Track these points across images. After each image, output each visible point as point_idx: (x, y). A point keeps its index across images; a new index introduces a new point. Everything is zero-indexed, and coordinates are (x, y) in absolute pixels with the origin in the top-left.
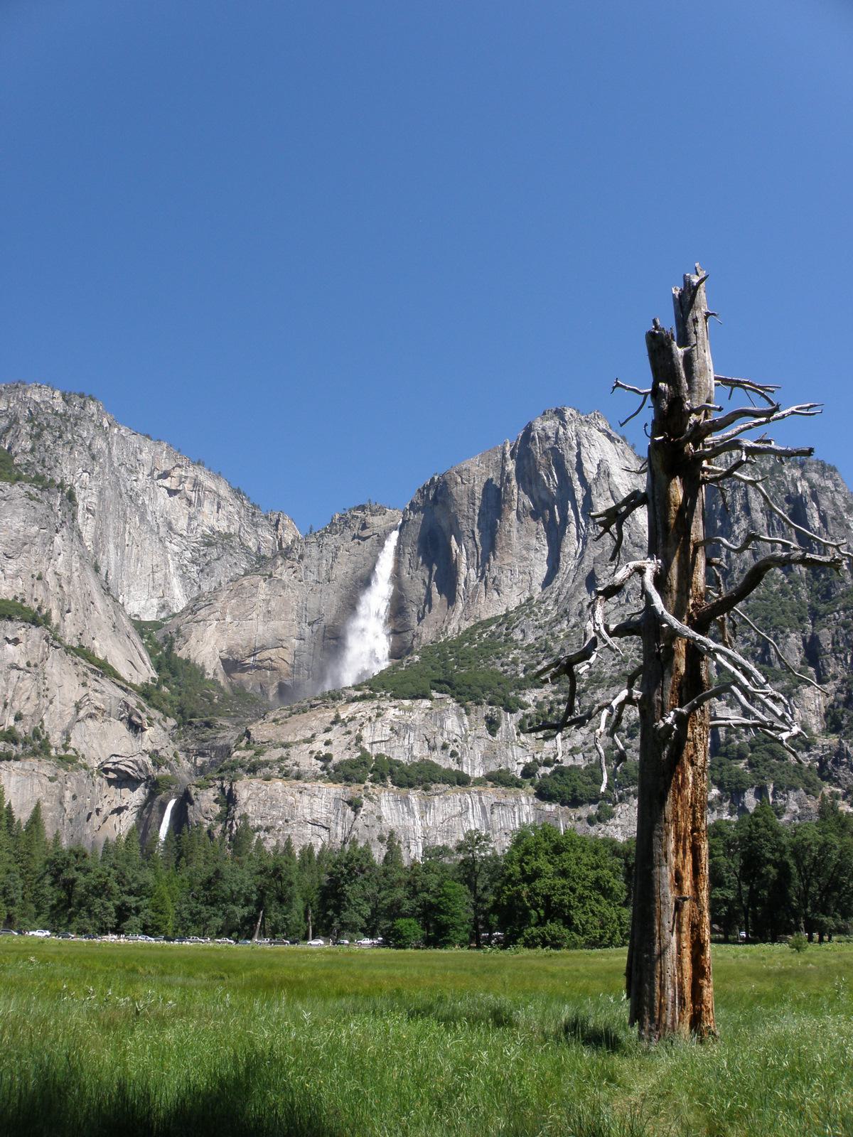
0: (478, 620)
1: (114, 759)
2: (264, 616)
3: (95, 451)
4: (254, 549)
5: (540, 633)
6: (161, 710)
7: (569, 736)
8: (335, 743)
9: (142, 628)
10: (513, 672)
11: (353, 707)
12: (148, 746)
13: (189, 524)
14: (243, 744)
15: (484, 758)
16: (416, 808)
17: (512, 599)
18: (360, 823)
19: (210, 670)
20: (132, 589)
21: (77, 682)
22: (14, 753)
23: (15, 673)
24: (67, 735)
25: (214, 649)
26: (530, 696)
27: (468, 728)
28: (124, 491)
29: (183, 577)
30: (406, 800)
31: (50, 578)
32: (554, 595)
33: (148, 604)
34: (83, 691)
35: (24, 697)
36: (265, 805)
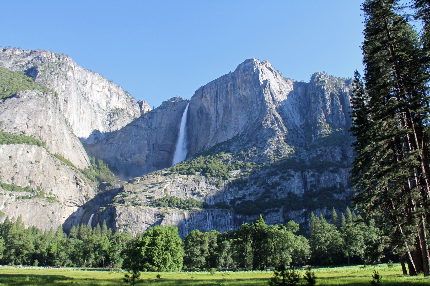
0: (217, 143)
4: (133, 115)
13: (107, 105)
31: (46, 127)
32: (246, 133)
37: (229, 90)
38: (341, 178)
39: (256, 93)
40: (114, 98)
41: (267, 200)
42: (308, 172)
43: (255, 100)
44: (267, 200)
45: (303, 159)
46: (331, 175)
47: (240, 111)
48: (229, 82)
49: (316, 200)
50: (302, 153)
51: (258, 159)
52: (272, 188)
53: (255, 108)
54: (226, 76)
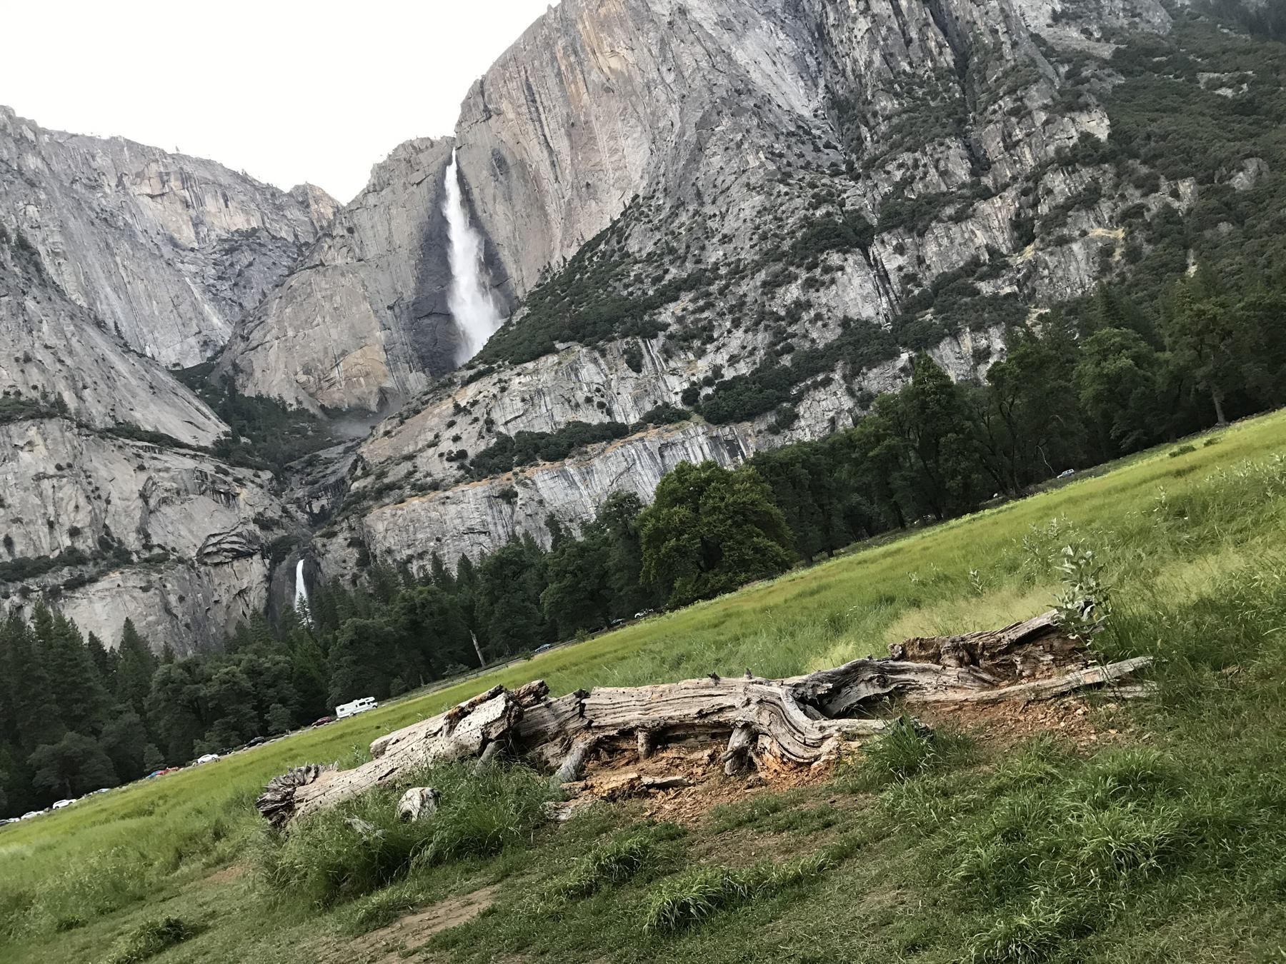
1: (214, 540)
2: (332, 317)
3: (29, 175)
4: (291, 239)
5: (658, 236)
6: (249, 466)
7: (724, 345)
8: (464, 437)
9: (190, 378)
10: (640, 293)
11: (472, 389)
12: (250, 513)
13: (197, 233)
14: (359, 472)
15: (636, 400)
16: (577, 478)
17: (612, 207)
18: (520, 515)
19: (290, 399)
20: (156, 335)
21: (130, 469)
22: (87, 576)
23: (46, 484)
24: (143, 532)
25: (287, 374)
26: (667, 314)
27: (607, 372)
28: (93, 215)
29: (216, 298)
30: (564, 474)
31: (40, 354)
32: (660, 186)
33: (185, 347)
34: (143, 476)
35: (71, 507)
36: (407, 531)
37: (563, 68)
38: (987, 229)
39: (650, 50)
40: (212, 204)
41: (786, 360)
42: (883, 242)
43: (655, 75)
44: (786, 360)
45: (855, 210)
46: (955, 229)
47: (620, 123)
48: (555, 43)
49: (929, 317)
50: (845, 191)
51: (721, 253)
52: (790, 324)
53: (663, 98)
54: (541, 22)
